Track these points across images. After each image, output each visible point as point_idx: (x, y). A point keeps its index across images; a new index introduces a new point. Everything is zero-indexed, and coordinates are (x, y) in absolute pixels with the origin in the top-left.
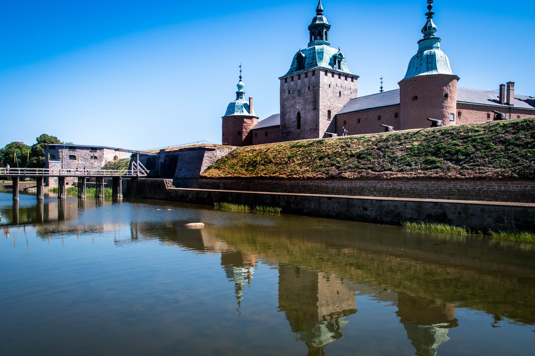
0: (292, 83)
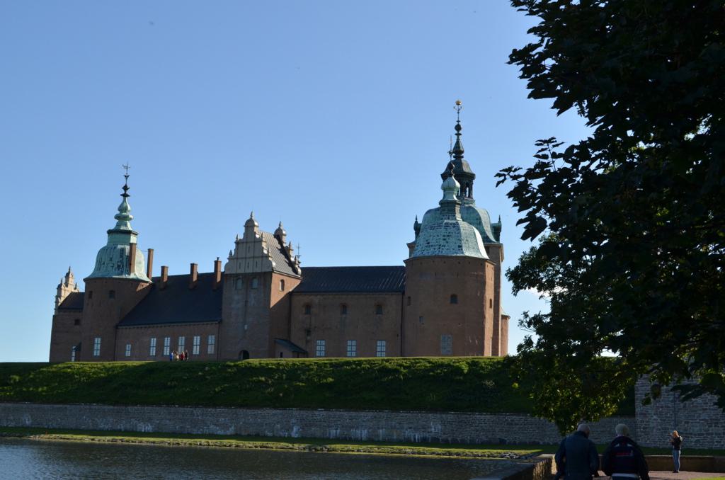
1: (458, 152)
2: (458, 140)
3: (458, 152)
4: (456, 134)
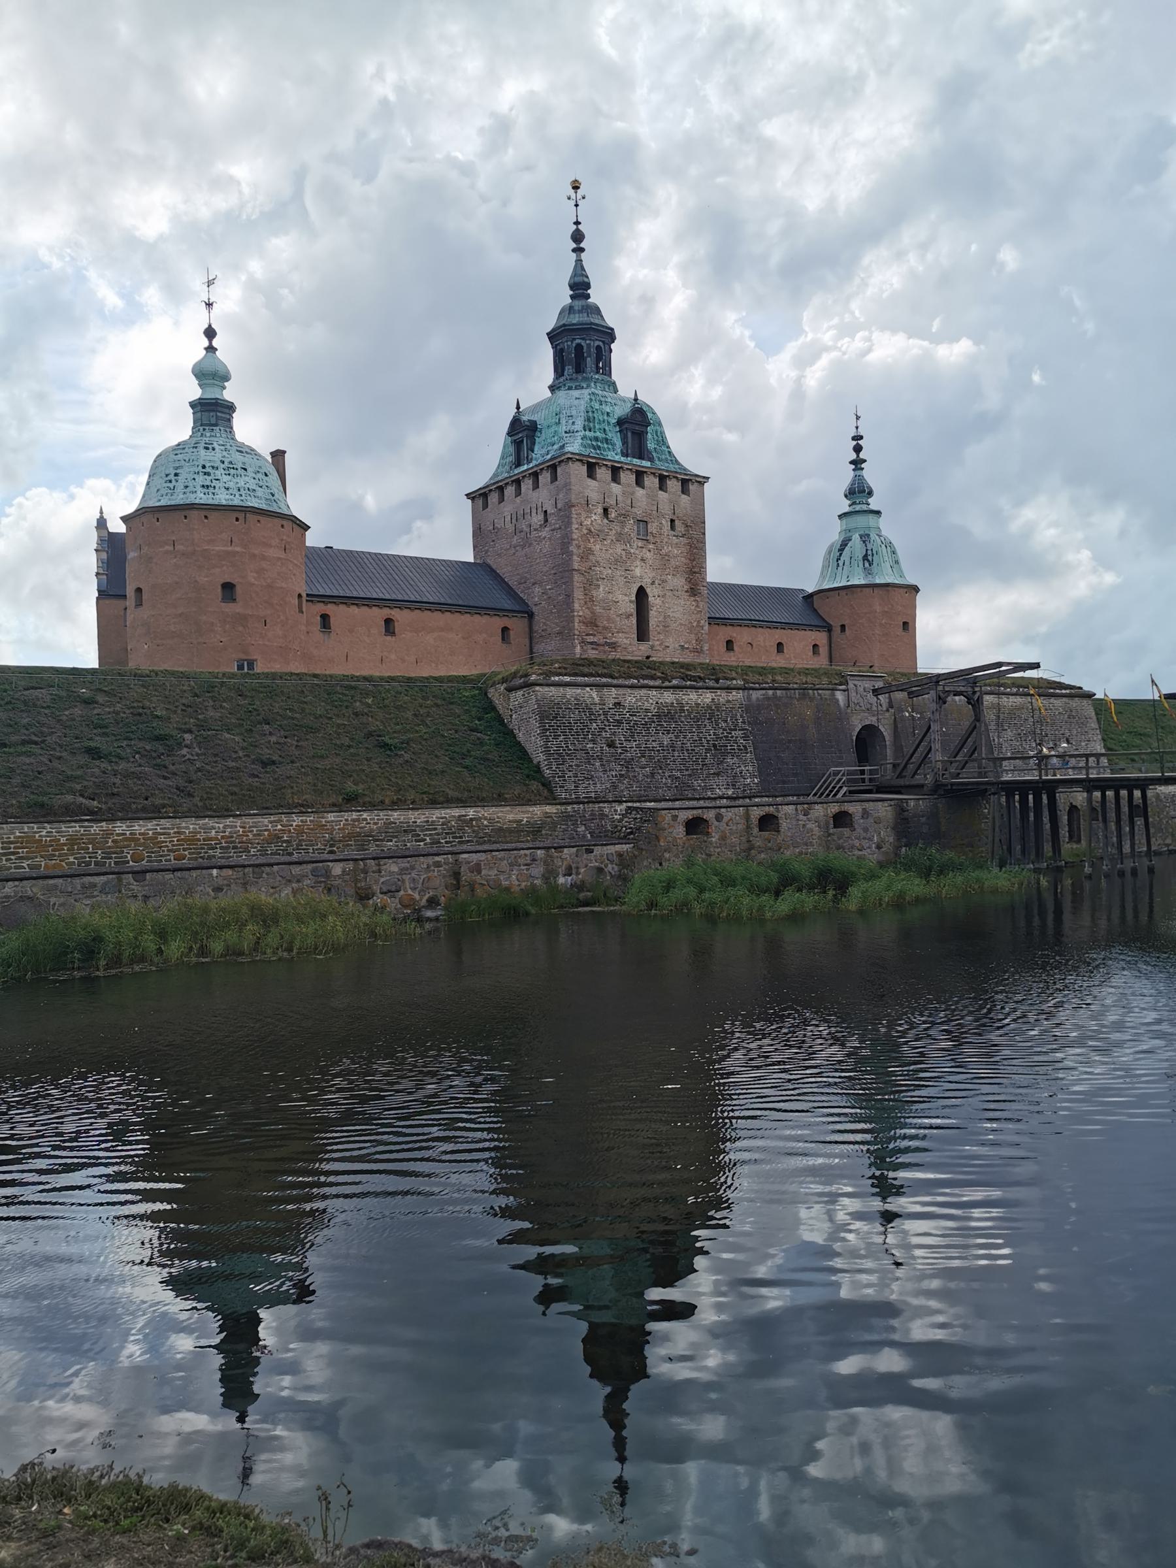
0: (616, 488)
1: (580, 287)
2: (579, 266)
3: (580, 287)
4: (574, 250)
